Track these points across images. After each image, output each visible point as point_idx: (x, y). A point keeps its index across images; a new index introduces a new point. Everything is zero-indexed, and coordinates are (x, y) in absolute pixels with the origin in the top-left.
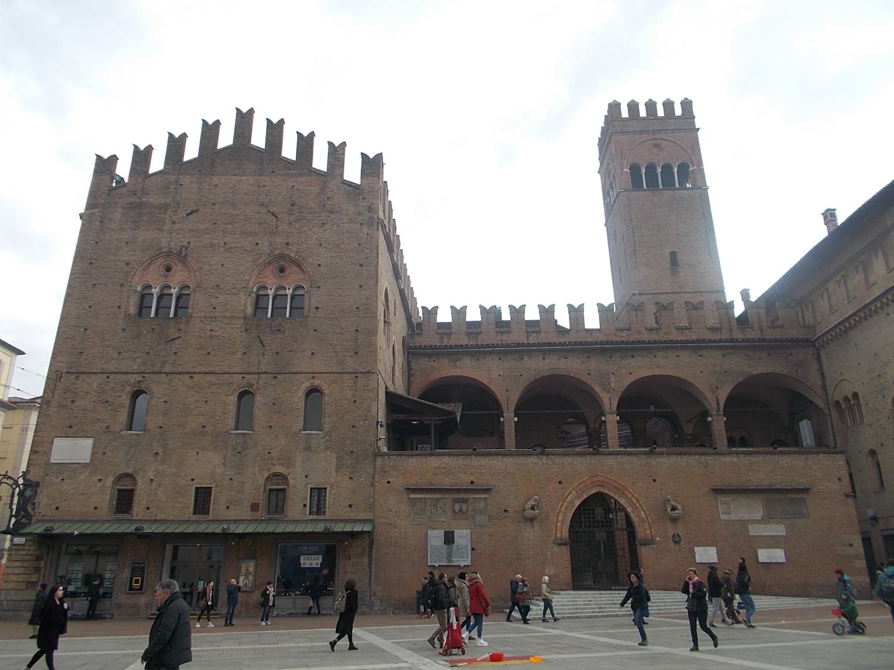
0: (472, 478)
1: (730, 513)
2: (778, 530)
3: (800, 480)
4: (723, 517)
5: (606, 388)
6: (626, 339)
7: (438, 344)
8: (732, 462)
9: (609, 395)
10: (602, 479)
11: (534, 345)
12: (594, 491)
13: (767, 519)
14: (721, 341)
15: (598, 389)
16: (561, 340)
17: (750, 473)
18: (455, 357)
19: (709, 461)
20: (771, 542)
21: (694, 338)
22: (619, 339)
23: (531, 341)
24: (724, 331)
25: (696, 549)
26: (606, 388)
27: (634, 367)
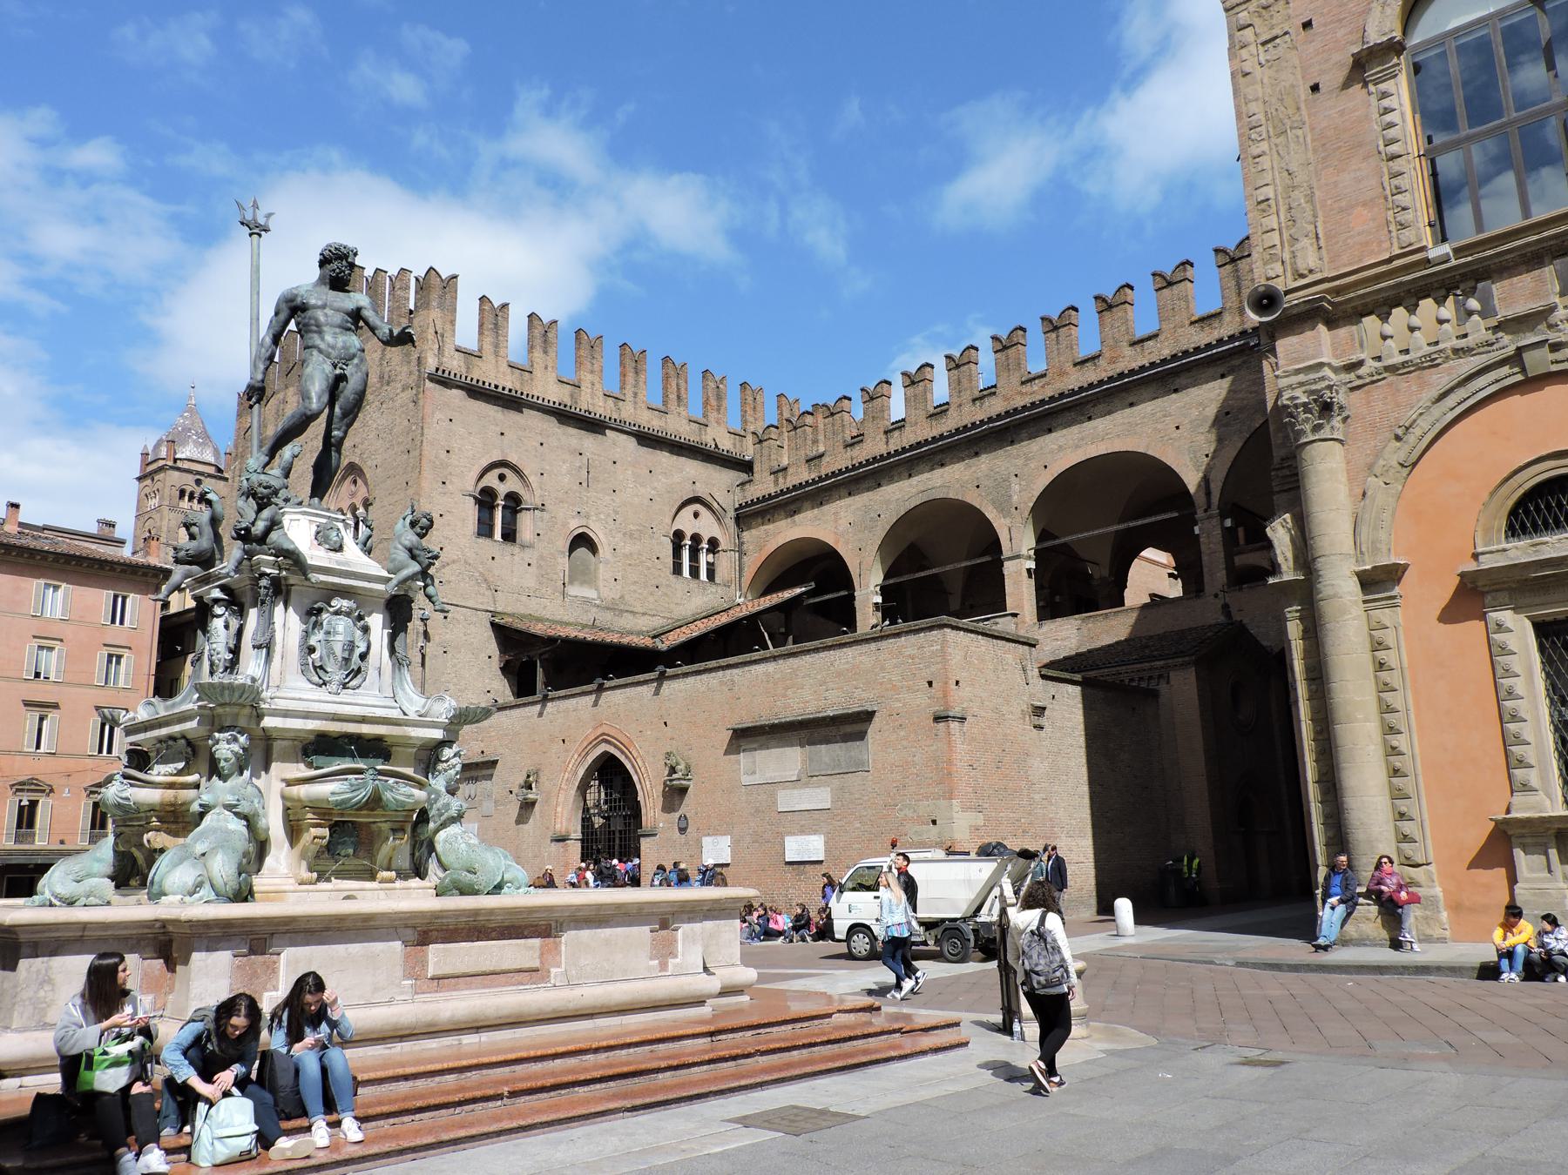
0: (482, 746)
1: (754, 773)
2: (818, 797)
3: (865, 695)
4: (746, 780)
5: (1004, 508)
6: (1037, 398)
7: (772, 492)
8: (767, 674)
9: (1008, 521)
10: (605, 729)
11: (897, 453)
12: (603, 748)
13: (809, 777)
14: (1220, 342)
15: (991, 514)
16: (935, 433)
17: (789, 692)
18: (793, 507)
19: (736, 678)
20: (806, 821)
21: (1166, 353)
22: (1027, 401)
23: (892, 449)
24: (1227, 317)
25: (706, 841)
26: (1004, 508)
27: (1052, 452)
